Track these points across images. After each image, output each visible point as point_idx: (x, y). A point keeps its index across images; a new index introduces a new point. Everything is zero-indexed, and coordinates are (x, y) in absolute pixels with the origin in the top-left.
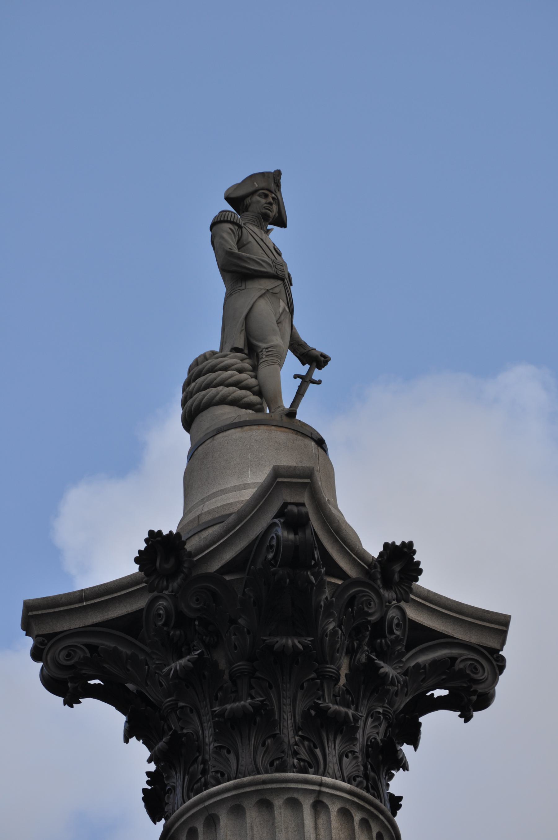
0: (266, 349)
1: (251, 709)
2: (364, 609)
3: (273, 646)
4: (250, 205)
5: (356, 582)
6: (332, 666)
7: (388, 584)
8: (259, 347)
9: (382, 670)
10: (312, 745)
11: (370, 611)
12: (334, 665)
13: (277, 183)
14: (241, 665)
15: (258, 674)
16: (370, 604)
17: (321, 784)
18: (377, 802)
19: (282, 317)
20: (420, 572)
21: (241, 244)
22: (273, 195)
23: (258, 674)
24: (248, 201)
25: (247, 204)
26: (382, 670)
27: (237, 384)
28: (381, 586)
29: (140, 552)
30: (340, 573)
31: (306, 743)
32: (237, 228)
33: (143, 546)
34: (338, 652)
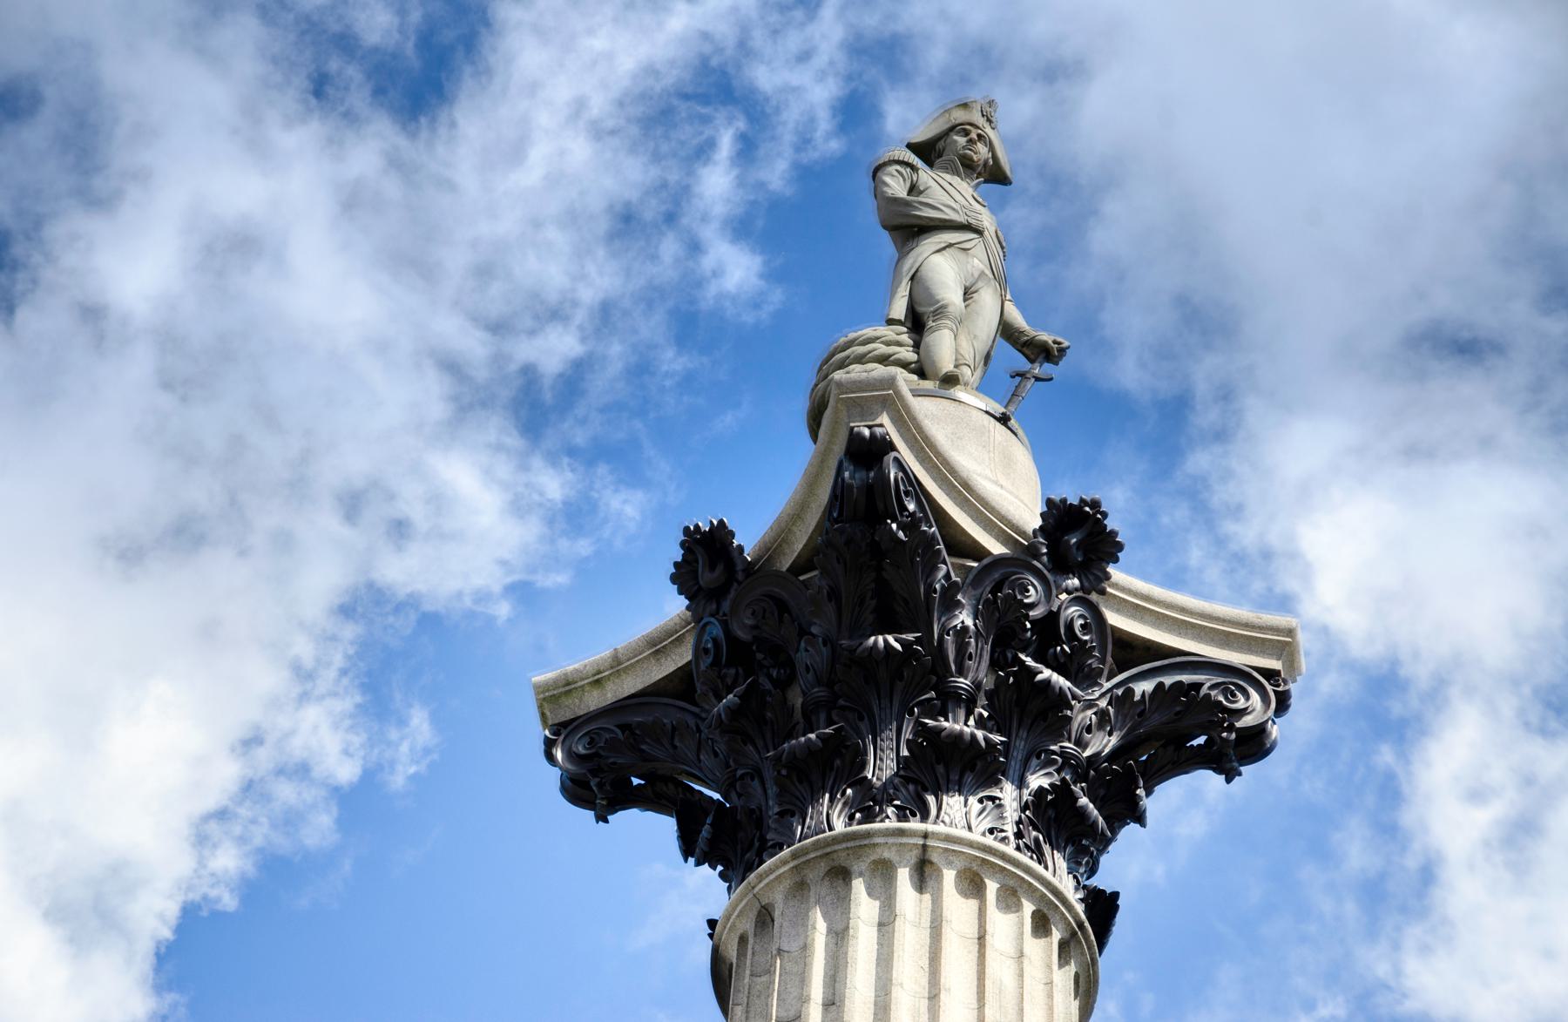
0: (934, 312)
1: (820, 744)
2: (1016, 597)
3: (856, 650)
4: (944, 150)
5: (1001, 560)
6: (961, 680)
7: (1062, 565)
8: (923, 314)
9: (1039, 677)
10: (919, 788)
11: (1026, 601)
12: (966, 679)
13: (987, 116)
14: (819, 692)
15: (841, 702)
16: (1028, 591)
17: (926, 836)
18: (1039, 869)
19: (980, 284)
20: (1120, 547)
21: (913, 189)
22: (980, 131)
23: (841, 702)
24: (941, 145)
25: (940, 150)
26: (1039, 677)
27: (884, 360)
28: (1050, 567)
29: (676, 565)
30: (977, 552)
31: (911, 787)
32: (908, 170)
33: (678, 555)
34: (970, 659)
